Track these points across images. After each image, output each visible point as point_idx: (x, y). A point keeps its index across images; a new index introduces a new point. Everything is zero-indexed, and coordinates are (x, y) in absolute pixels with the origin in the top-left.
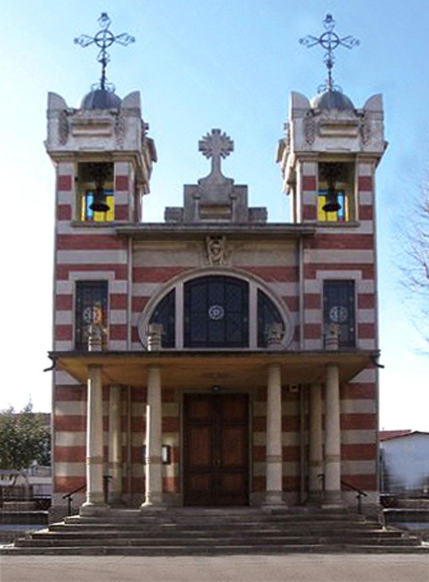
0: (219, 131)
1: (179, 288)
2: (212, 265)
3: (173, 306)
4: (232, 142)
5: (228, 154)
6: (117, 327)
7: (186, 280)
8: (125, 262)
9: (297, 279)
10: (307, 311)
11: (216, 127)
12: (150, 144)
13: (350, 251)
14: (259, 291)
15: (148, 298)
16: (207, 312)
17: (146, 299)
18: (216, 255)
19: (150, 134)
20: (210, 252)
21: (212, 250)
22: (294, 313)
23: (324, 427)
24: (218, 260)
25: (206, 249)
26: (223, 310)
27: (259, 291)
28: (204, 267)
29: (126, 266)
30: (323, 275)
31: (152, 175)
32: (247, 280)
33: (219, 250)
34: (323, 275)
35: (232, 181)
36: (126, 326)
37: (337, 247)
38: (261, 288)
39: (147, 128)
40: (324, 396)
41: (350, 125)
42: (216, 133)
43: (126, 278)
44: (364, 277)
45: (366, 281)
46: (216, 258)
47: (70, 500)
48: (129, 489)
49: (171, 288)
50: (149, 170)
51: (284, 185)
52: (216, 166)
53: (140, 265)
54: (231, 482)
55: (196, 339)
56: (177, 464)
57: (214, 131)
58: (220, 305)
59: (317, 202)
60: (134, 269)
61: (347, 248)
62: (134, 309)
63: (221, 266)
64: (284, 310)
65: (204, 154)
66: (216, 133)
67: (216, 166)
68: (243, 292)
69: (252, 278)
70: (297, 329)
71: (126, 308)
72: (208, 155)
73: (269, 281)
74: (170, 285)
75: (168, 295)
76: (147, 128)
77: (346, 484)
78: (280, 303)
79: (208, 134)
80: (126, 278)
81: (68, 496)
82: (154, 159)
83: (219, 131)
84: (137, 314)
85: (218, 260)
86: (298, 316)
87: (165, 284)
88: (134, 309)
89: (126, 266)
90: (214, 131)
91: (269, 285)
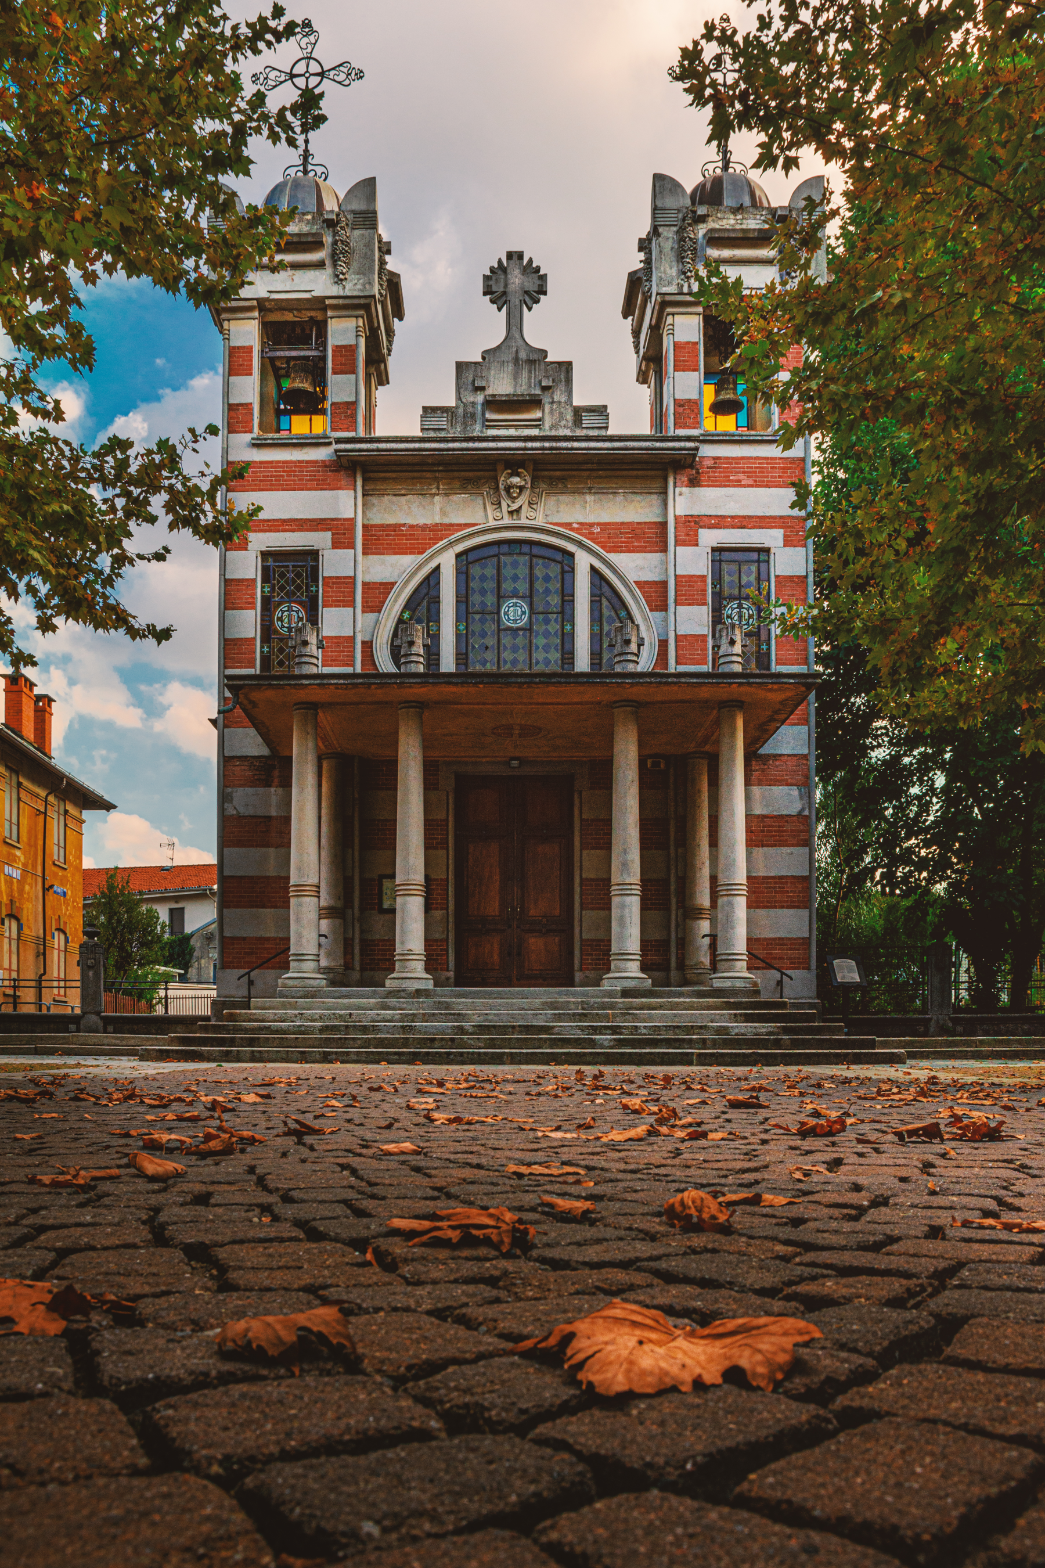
0: (520, 255)
1: (447, 561)
2: (507, 521)
3: (436, 601)
4: (543, 278)
5: (537, 301)
6: (338, 640)
7: (460, 548)
8: (350, 515)
9: (664, 549)
10: (681, 609)
11: (515, 248)
12: (393, 284)
13: (618, 519)
14: (593, 568)
15: (393, 584)
16: (498, 613)
17: (388, 586)
18: (513, 499)
19: (392, 264)
20: (503, 493)
21: (508, 489)
22: (658, 615)
23: (714, 843)
24: (518, 511)
25: (497, 488)
26: (526, 608)
27: (593, 568)
28: (492, 523)
29: (352, 521)
30: (710, 538)
31: (396, 340)
32: (571, 547)
33: (521, 488)
34: (710, 538)
35: (544, 353)
36: (352, 639)
37: (738, 484)
38: (598, 564)
39: (389, 252)
40: (714, 783)
41: (761, 239)
42: (515, 257)
43: (352, 546)
44: (788, 543)
45: (790, 550)
46: (515, 507)
47: (251, 983)
48: (357, 965)
49: (433, 564)
50: (390, 333)
51: (631, 362)
52: (515, 324)
53: (372, 522)
54: (492, 950)
55: (555, 656)
56: (338, 921)
57: (510, 255)
58: (522, 598)
59: (700, 393)
60: (365, 527)
61: (756, 485)
62: (367, 608)
63: (523, 521)
64: (637, 605)
65: (492, 301)
66: (515, 257)
67: (515, 324)
68: (563, 572)
69: (580, 544)
70: (663, 644)
71: (352, 604)
72: (500, 303)
73: (616, 549)
74: (431, 558)
75: (427, 578)
76: (389, 252)
77: (757, 958)
78: (631, 591)
79: (500, 261)
80: (352, 546)
81: (248, 973)
82: (399, 314)
83: (520, 255)
84: (372, 616)
85: (518, 511)
86: (666, 620)
87: (420, 558)
88: (367, 608)
89: (352, 521)
90: (510, 255)
91: (612, 557)
